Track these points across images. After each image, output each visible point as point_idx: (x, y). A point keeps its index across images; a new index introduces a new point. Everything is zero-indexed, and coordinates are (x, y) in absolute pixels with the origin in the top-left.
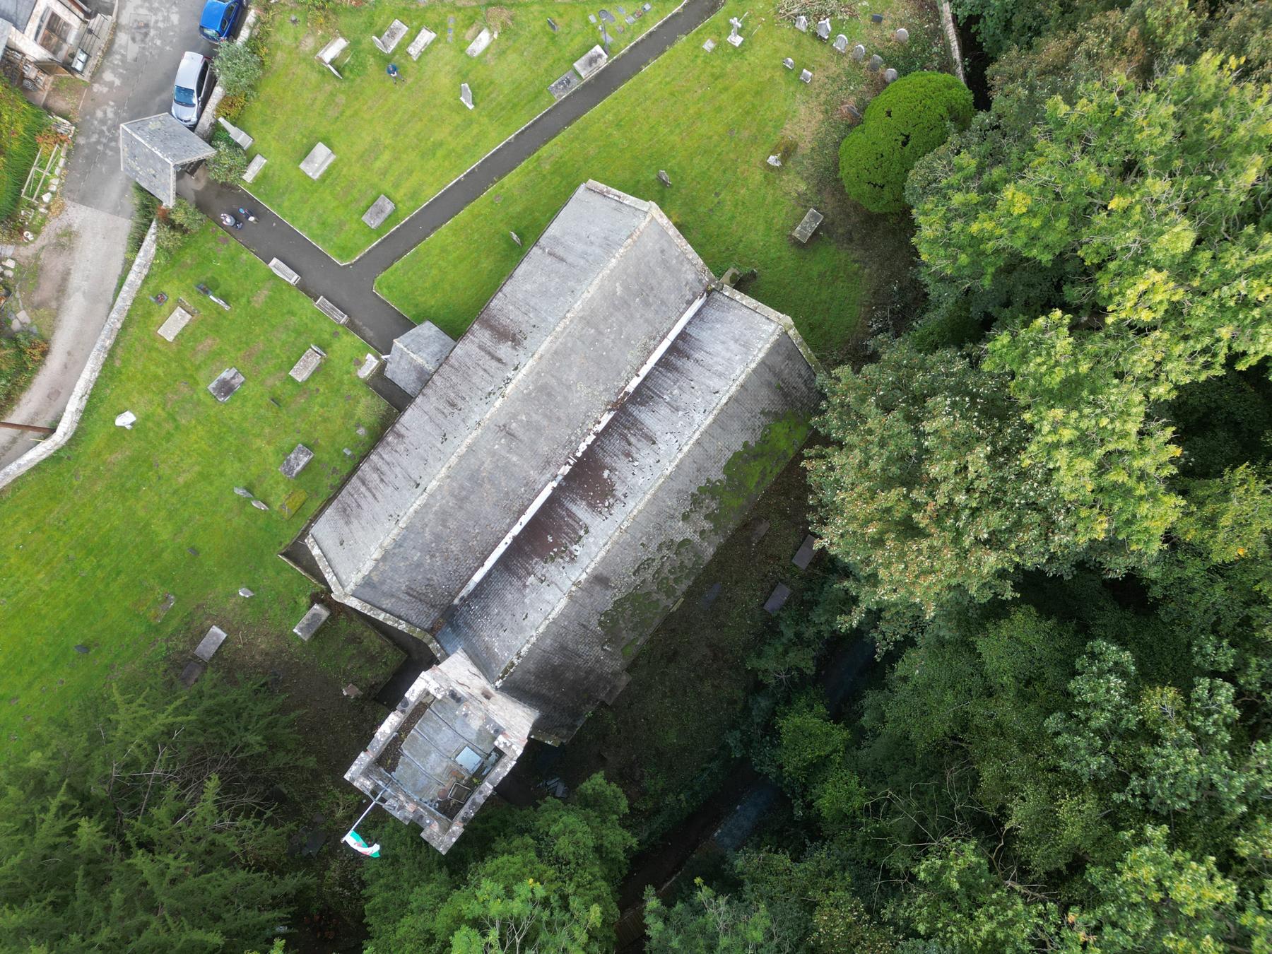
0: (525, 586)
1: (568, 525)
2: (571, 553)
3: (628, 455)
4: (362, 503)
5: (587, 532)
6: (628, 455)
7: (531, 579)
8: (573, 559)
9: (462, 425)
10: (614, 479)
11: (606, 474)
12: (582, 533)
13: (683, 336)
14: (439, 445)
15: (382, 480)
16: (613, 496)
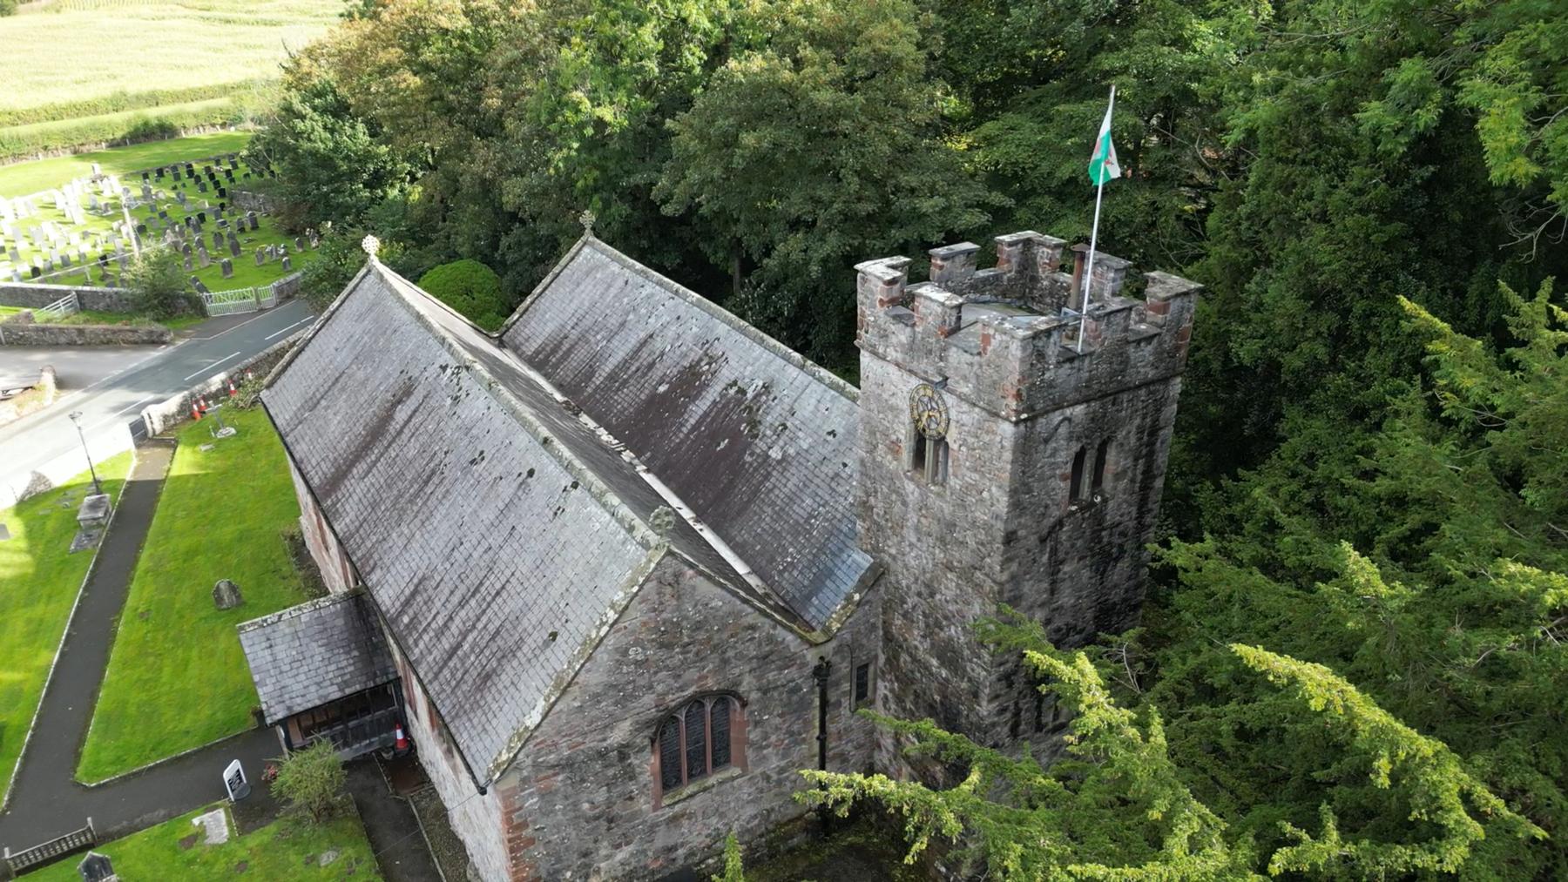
0: (784, 459)
1: (713, 420)
2: (757, 396)
3: (651, 366)
4: (491, 628)
5: (735, 383)
6: (651, 366)
7: (775, 454)
8: (766, 388)
9: (474, 432)
10: (675, 371)
11: (662, 389)
12: (732, 391)
13: (531, 362)
14: (484, 463)
15: (473, 595)
16: (701, 360)
